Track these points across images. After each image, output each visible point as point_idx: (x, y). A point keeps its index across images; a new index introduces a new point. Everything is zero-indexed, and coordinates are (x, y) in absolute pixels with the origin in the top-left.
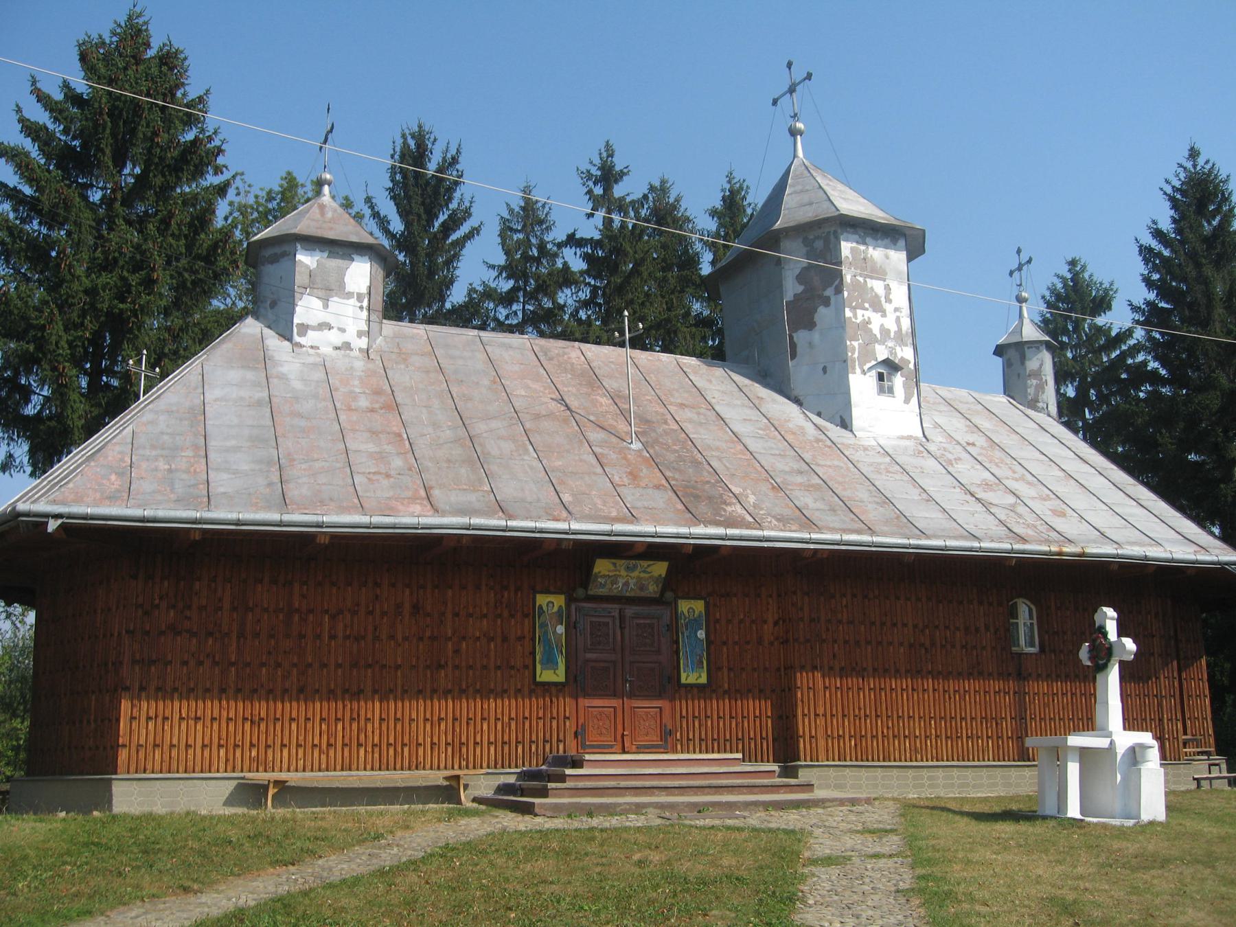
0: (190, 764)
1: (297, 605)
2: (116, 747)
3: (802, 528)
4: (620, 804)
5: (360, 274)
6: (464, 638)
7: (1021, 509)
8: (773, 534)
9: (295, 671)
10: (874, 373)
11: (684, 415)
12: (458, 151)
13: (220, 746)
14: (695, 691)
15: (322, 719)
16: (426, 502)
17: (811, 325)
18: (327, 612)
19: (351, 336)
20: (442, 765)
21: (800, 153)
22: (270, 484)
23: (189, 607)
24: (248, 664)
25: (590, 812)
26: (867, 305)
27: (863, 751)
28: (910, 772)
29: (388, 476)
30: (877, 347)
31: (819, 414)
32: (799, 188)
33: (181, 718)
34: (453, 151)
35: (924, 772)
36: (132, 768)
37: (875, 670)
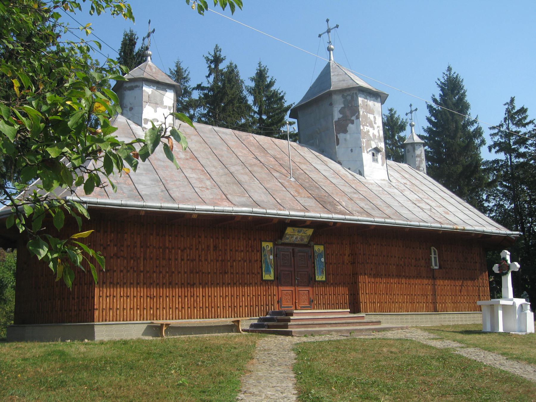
0: (125, 317)
1: (167, 245)
2: (93, 310)
3: (368, 216)
4: (322, 331)
5: (169, 98)
6: (234, 261)
7: (433, 210)
8: (360, 218)
9: (167, 274)
10: (371, 153)
11: (303, 167)
13: (137, 309)
14: (321, 284)
15: (179, 296)
16: (227, 201)
17: (345, 131)
18: (179, 248)
20: (227, 316)
21: (332, 58)
22: (162, 191)
23: (123, 246)
24: (148, 272)
25: (312, 334)
27: (383, 308)
28: (399, 317)
29: (207, 189)
30: (372, 142)
31: (349, 169)
32: (336, 73)
33: (121, 296)
35: (404, 317)
36: (101, 320)
37: (385, 275)
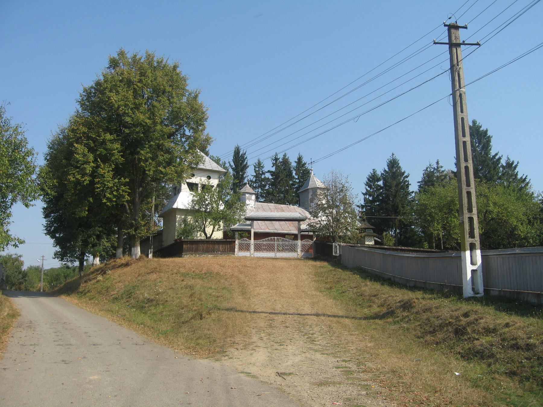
5: (254, 197)
19: (253, 205)
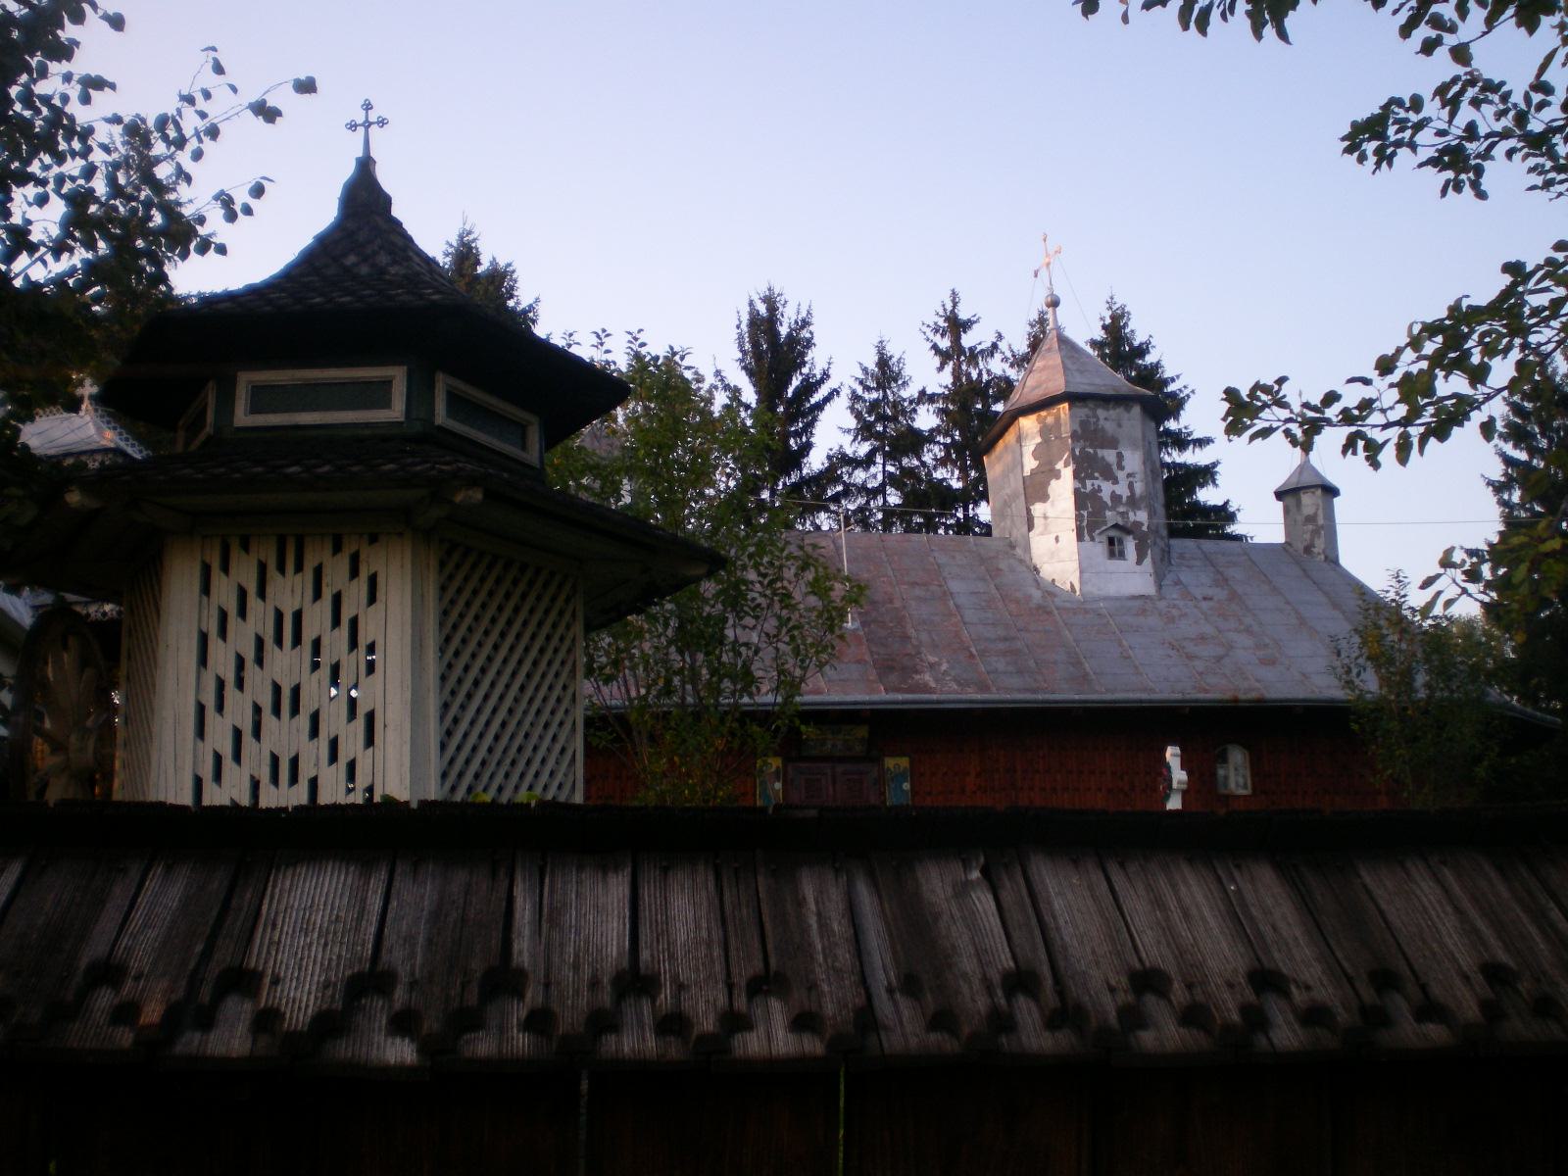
10: (1104, 538)
12: (809, 313)
17: (1044, 497)
26: (1096, 475)
30: (1108, 513)
34: (804, 314)
